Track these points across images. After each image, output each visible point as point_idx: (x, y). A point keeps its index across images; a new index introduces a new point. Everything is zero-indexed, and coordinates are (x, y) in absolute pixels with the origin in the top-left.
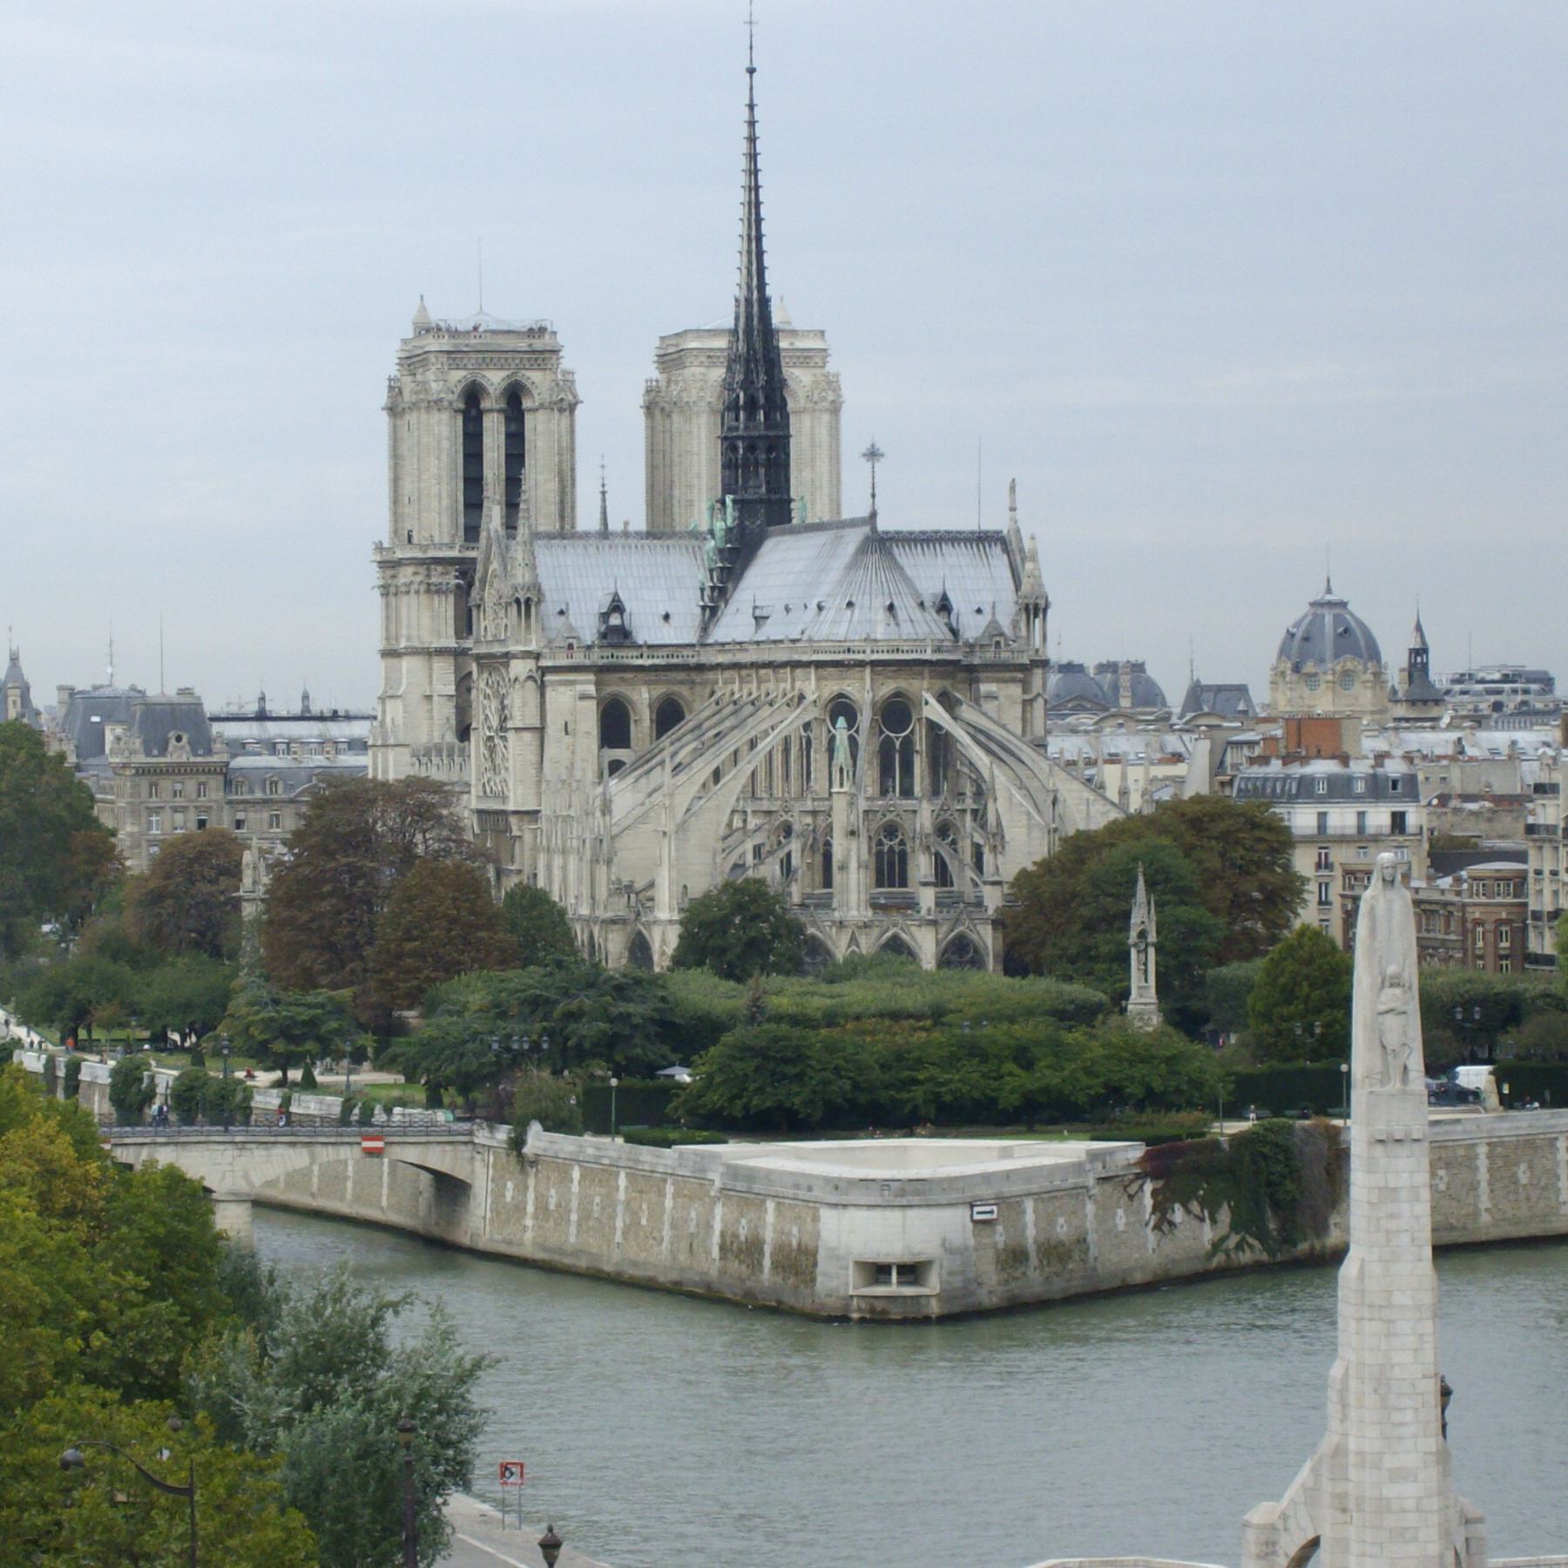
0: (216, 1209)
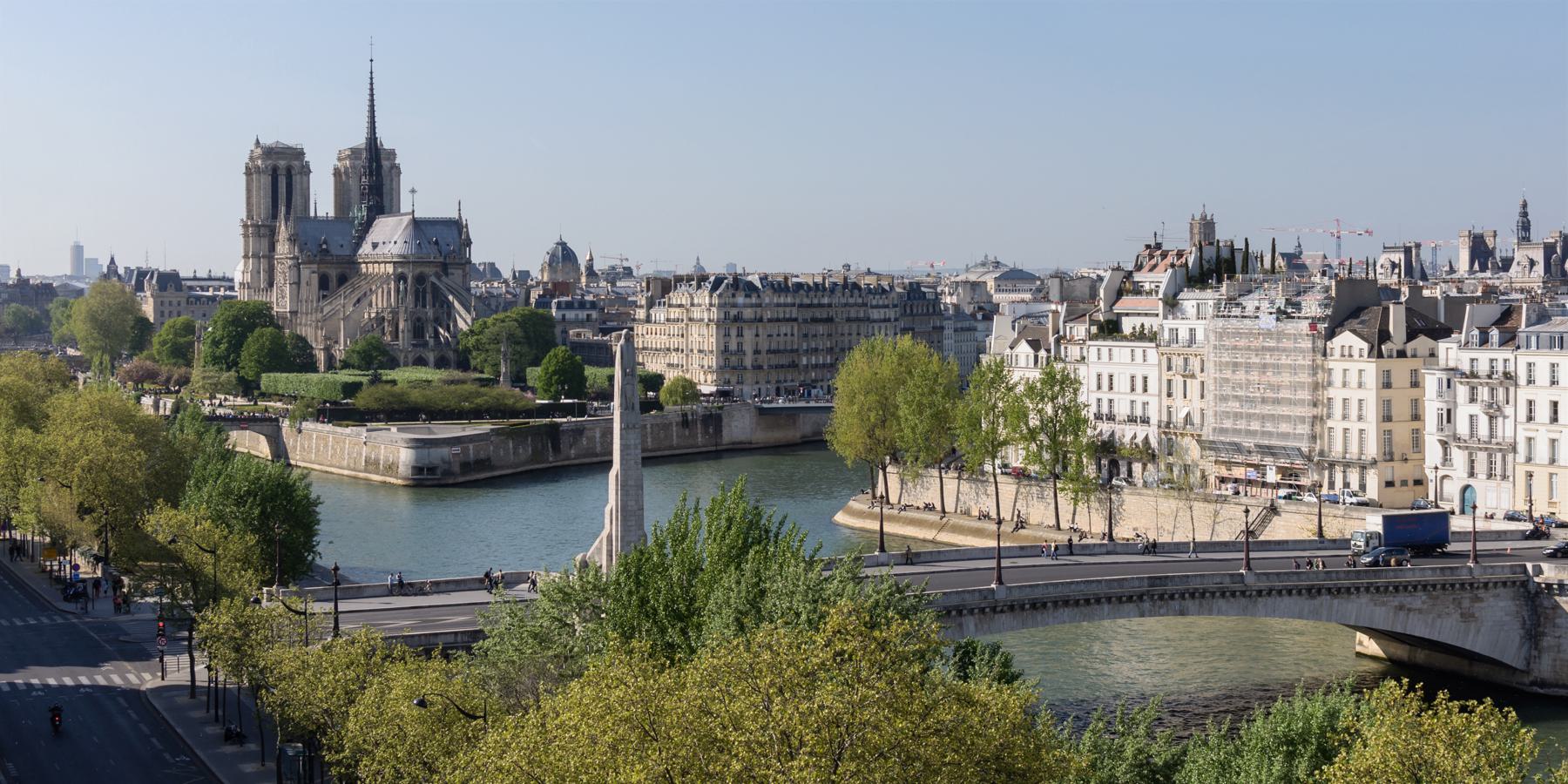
0: (410, 472)
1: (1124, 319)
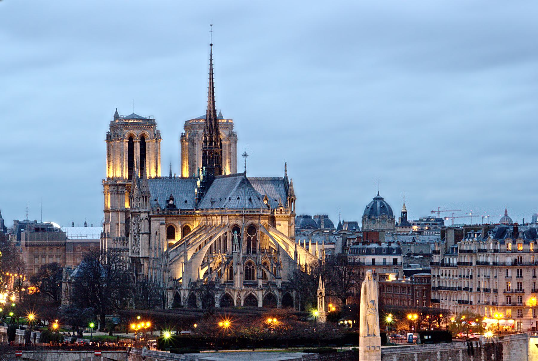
1: (63, 284)
